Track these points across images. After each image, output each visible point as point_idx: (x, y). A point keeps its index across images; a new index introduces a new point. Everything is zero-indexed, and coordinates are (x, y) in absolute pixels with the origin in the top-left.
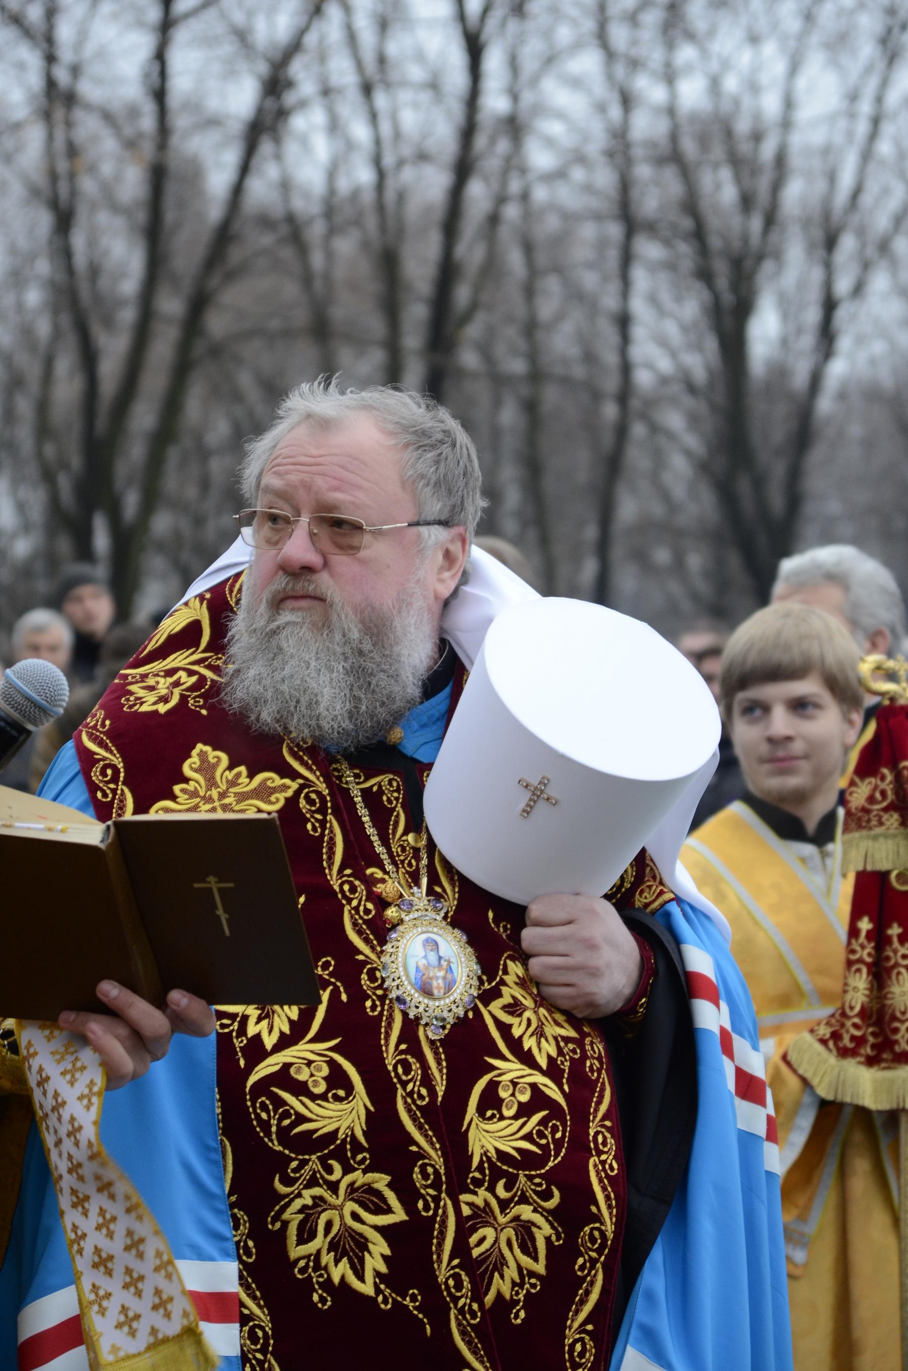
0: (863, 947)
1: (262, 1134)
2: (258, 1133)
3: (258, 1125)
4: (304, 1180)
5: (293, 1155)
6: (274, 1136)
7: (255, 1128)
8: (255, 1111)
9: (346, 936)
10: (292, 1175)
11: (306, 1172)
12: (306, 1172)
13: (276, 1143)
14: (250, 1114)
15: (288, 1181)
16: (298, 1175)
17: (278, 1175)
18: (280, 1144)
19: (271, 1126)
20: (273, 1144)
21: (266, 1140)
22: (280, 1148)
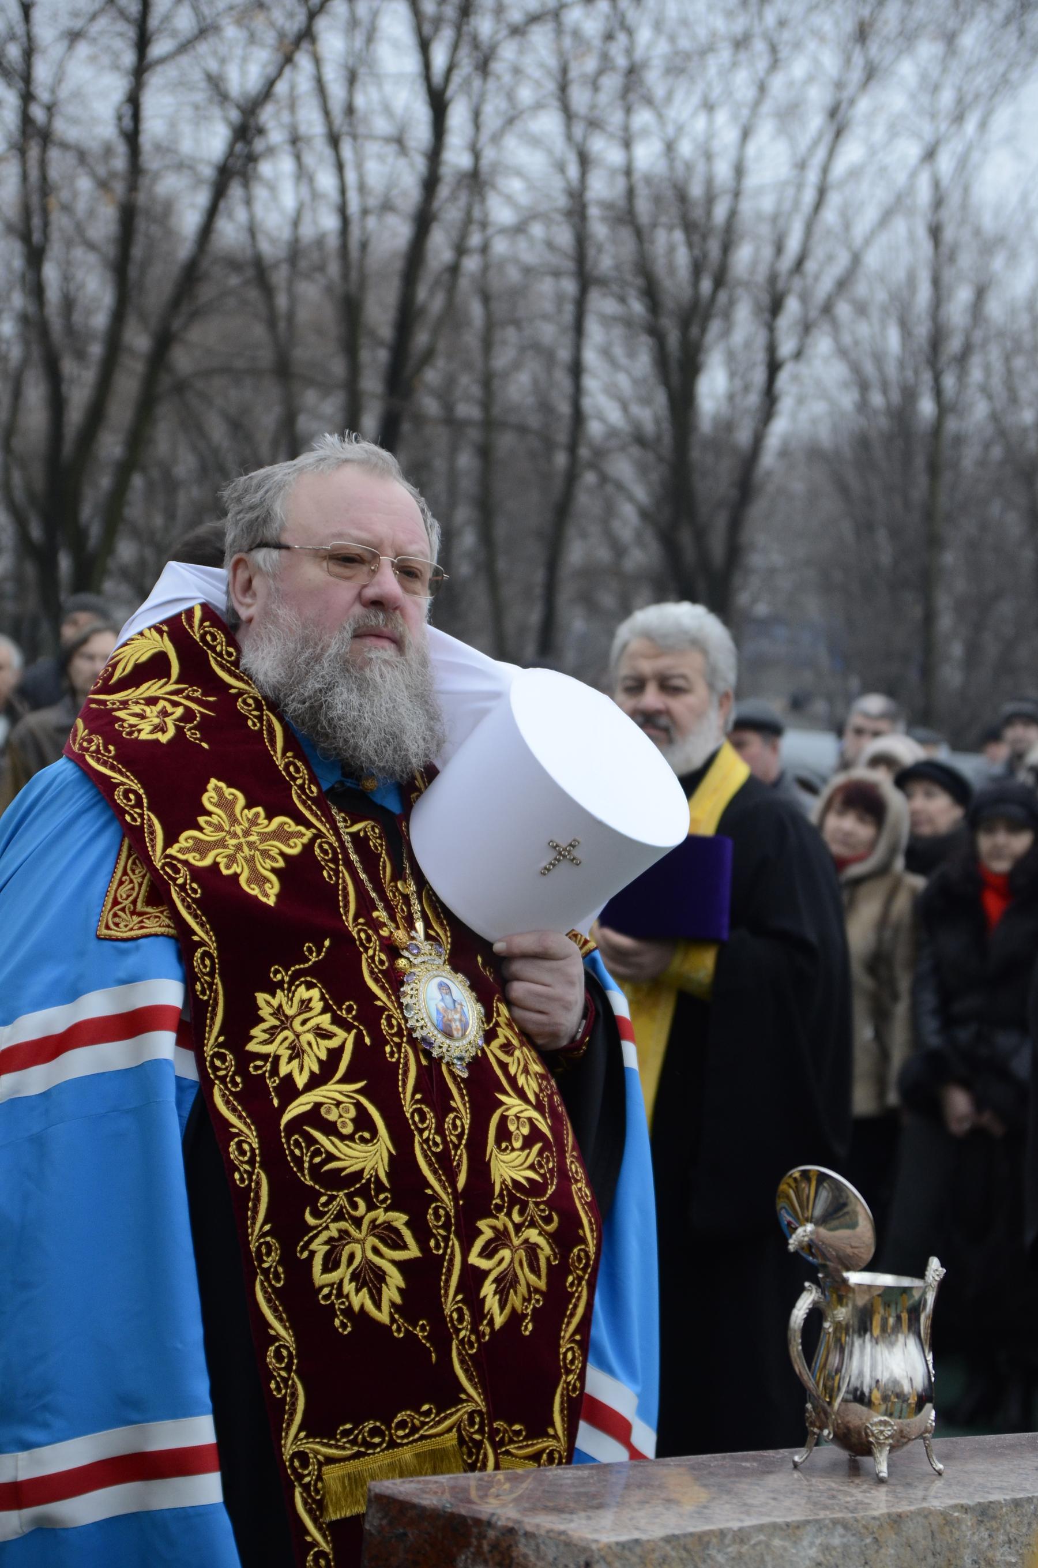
1: (295, 1169)
2: (292, 1168)
3: (292, 1160)
4: (332, 1214)
5: (322, 1190)
6: (306, 1172)
7: (289, 1163)
8: (289, 1148)
9: (365, 982)
10: (321, 1208)
11: (334, 1207)
12: (334, 1207)
13: (307, 1177)
14: (285, 1150)
15: (317, 1214)
16: (326, 1209)
17: (308, 1208)
18: (312, 1179)
19: (303, 1162)
20: (305, 1179)
21: (299, 1174)
22: (310, 1183)
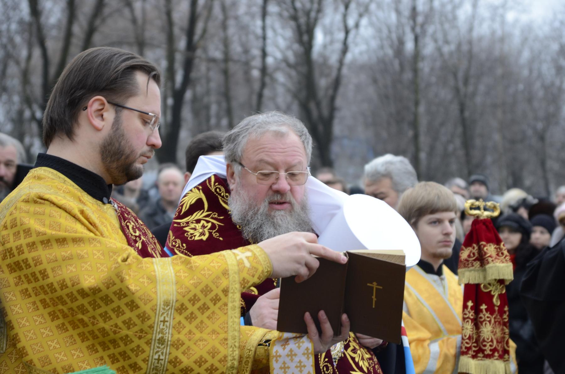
0: (469, 312)
